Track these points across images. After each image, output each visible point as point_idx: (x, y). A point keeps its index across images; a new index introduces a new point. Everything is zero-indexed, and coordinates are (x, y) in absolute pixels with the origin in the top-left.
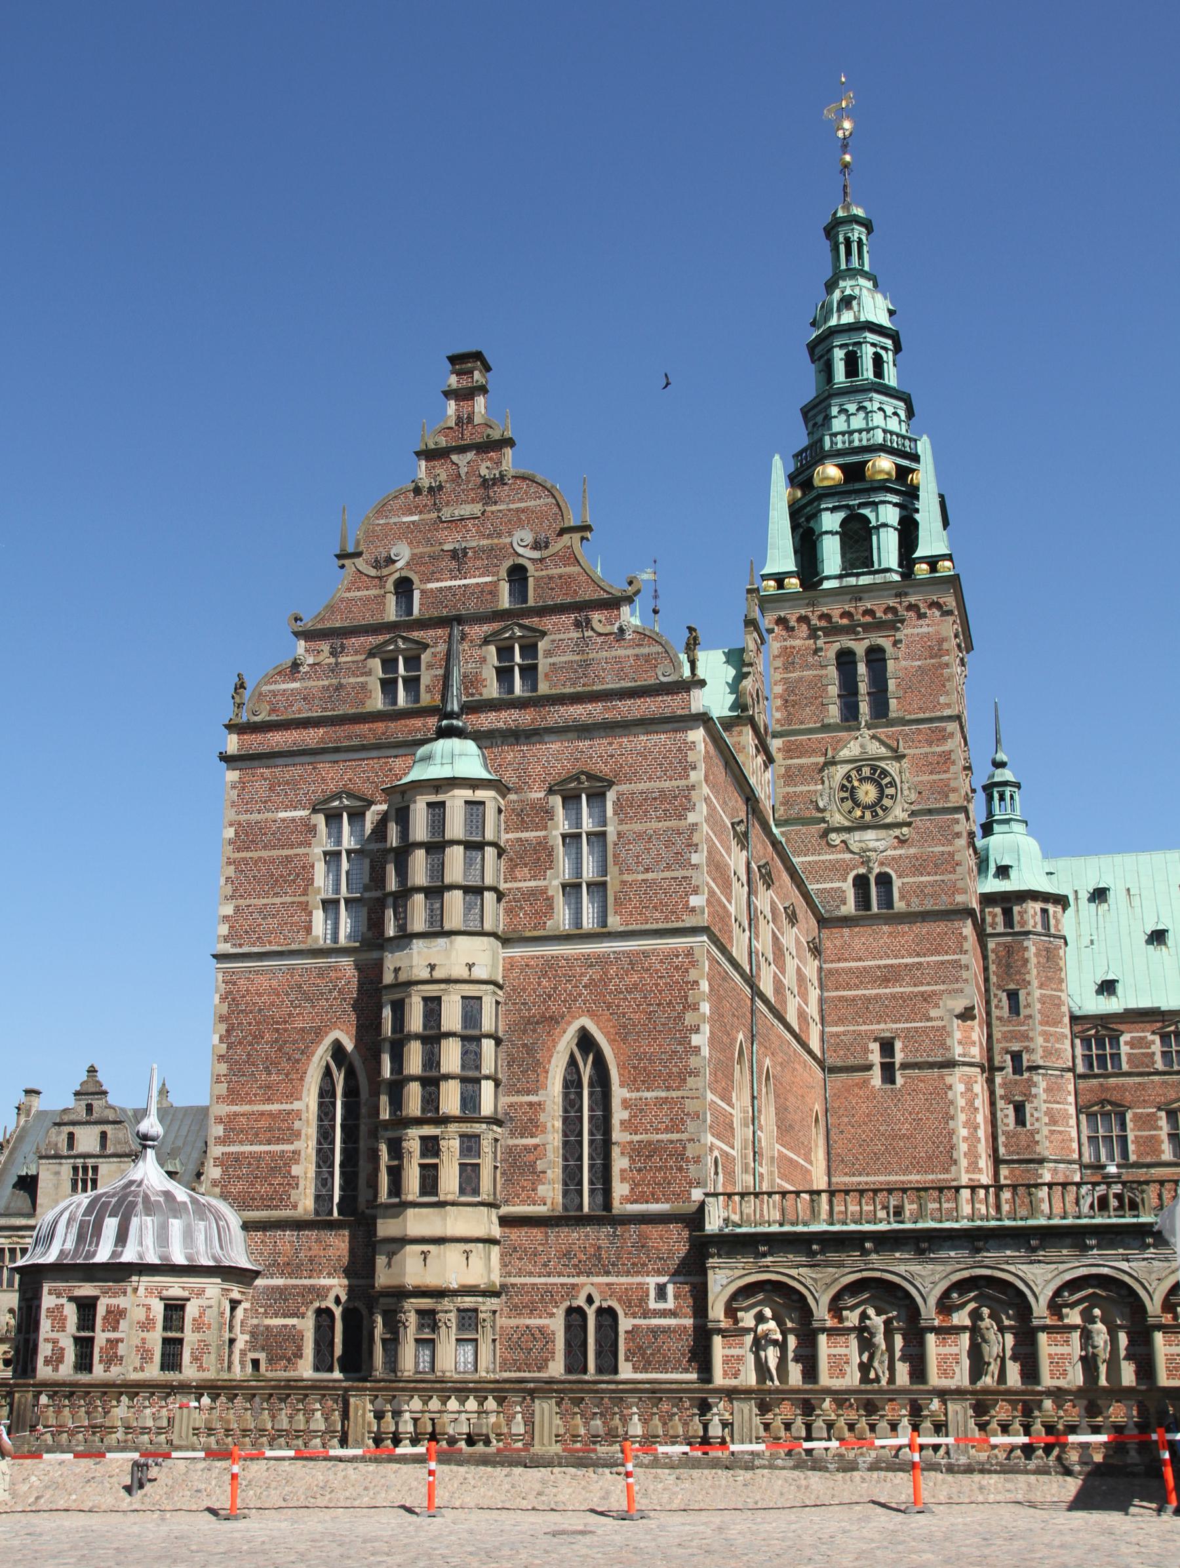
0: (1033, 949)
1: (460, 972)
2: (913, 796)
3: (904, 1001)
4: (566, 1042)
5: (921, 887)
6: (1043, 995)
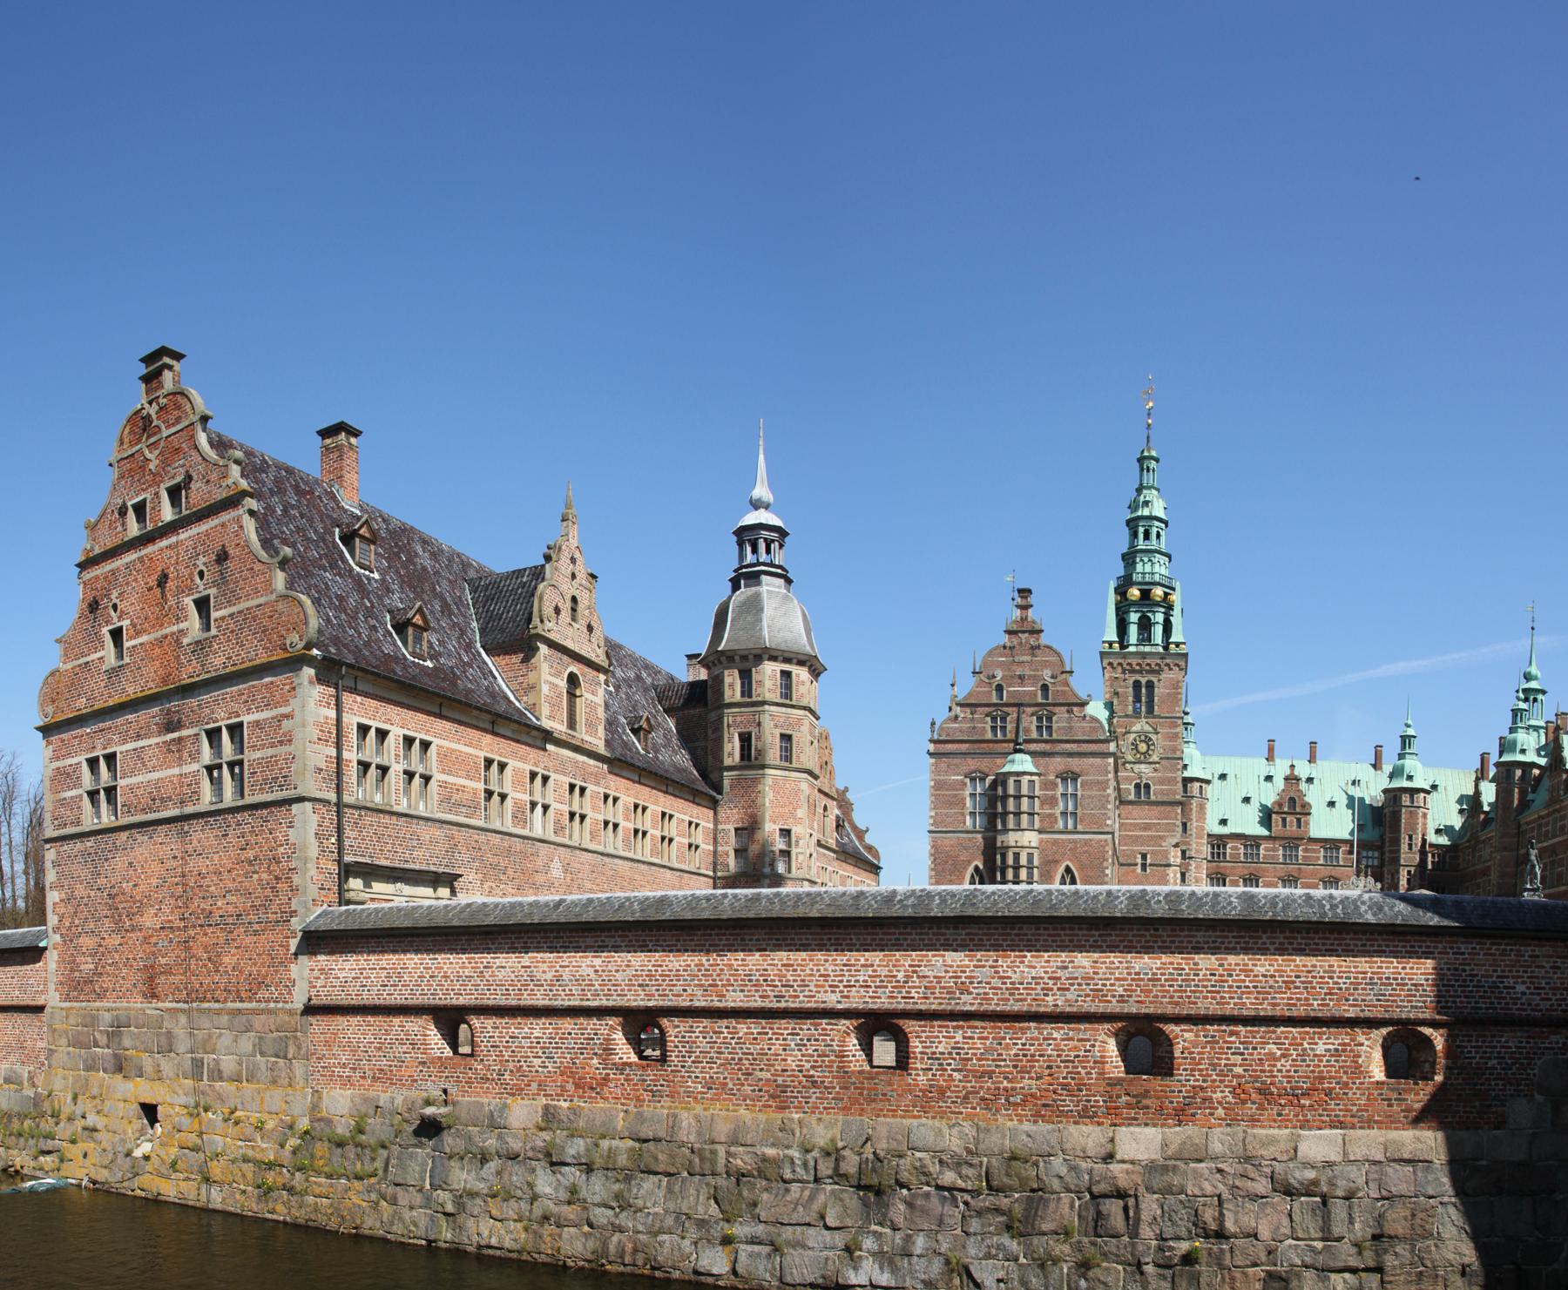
1: (1027, 844)
2: (1162, 751)
4: (1061, 870)
5: (1162, 790)
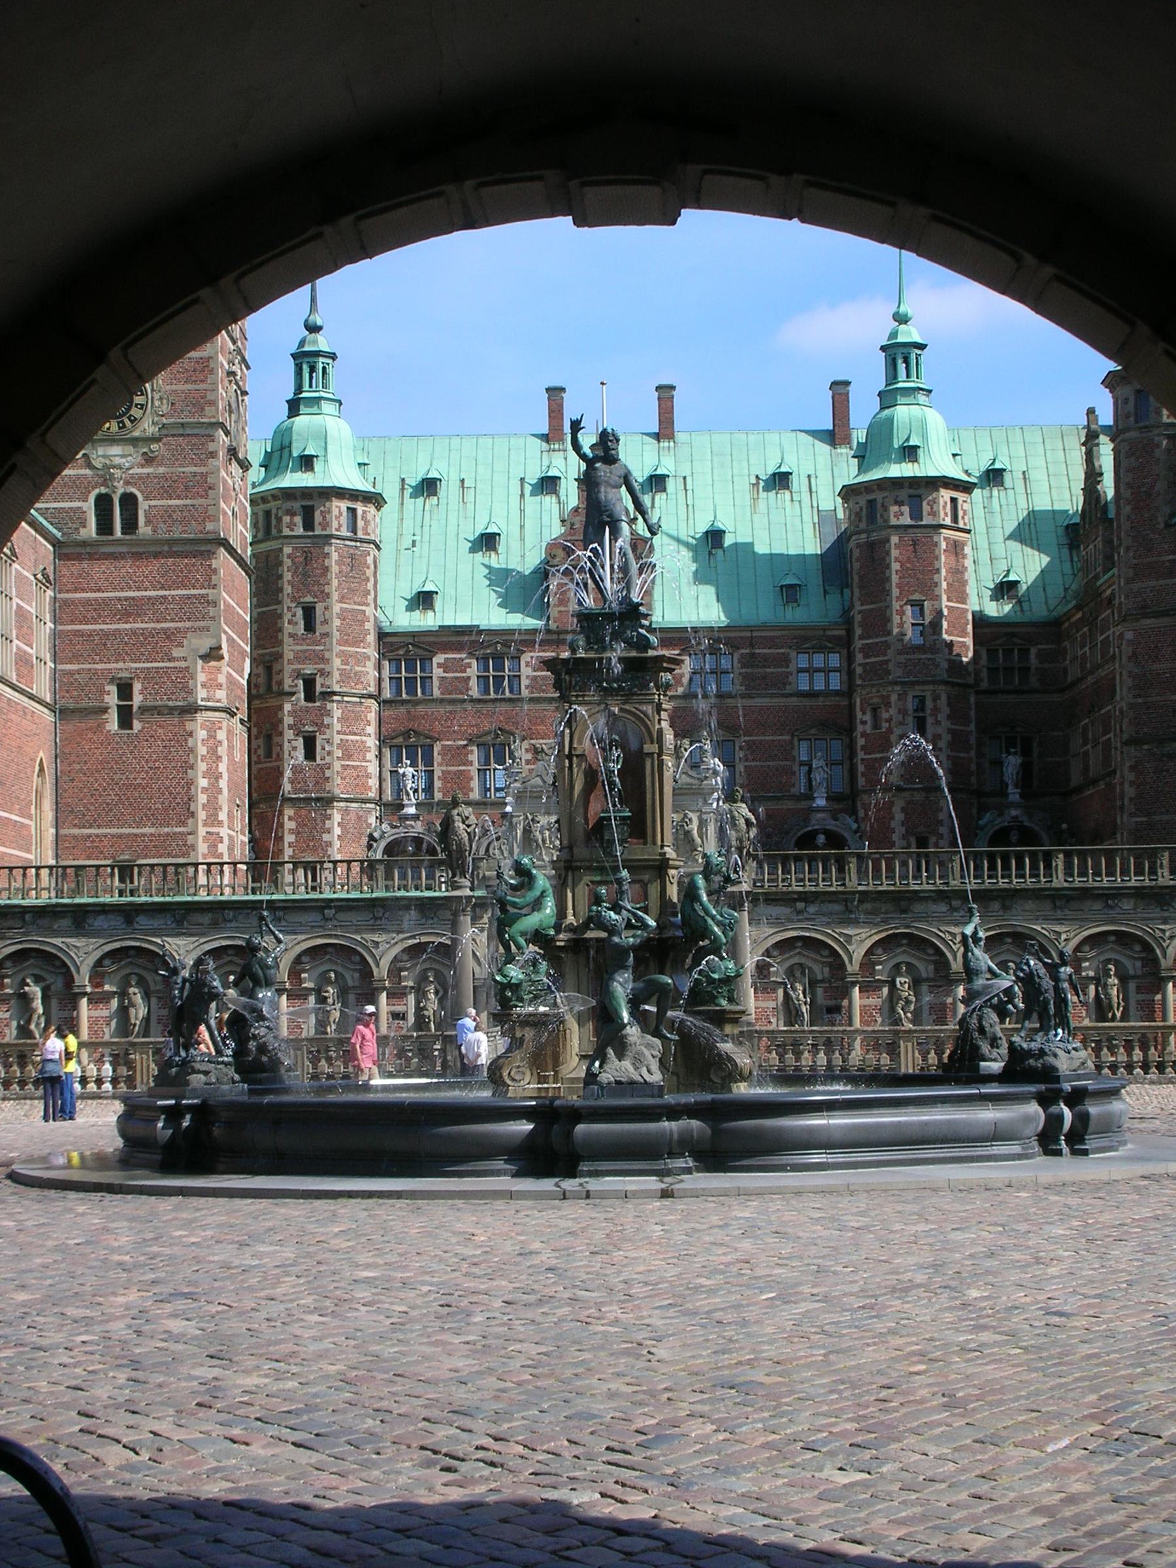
0: (335, 556)
2: (165, 408)
3: (145, 639)
5: (168, 512)
6: (341, 608)
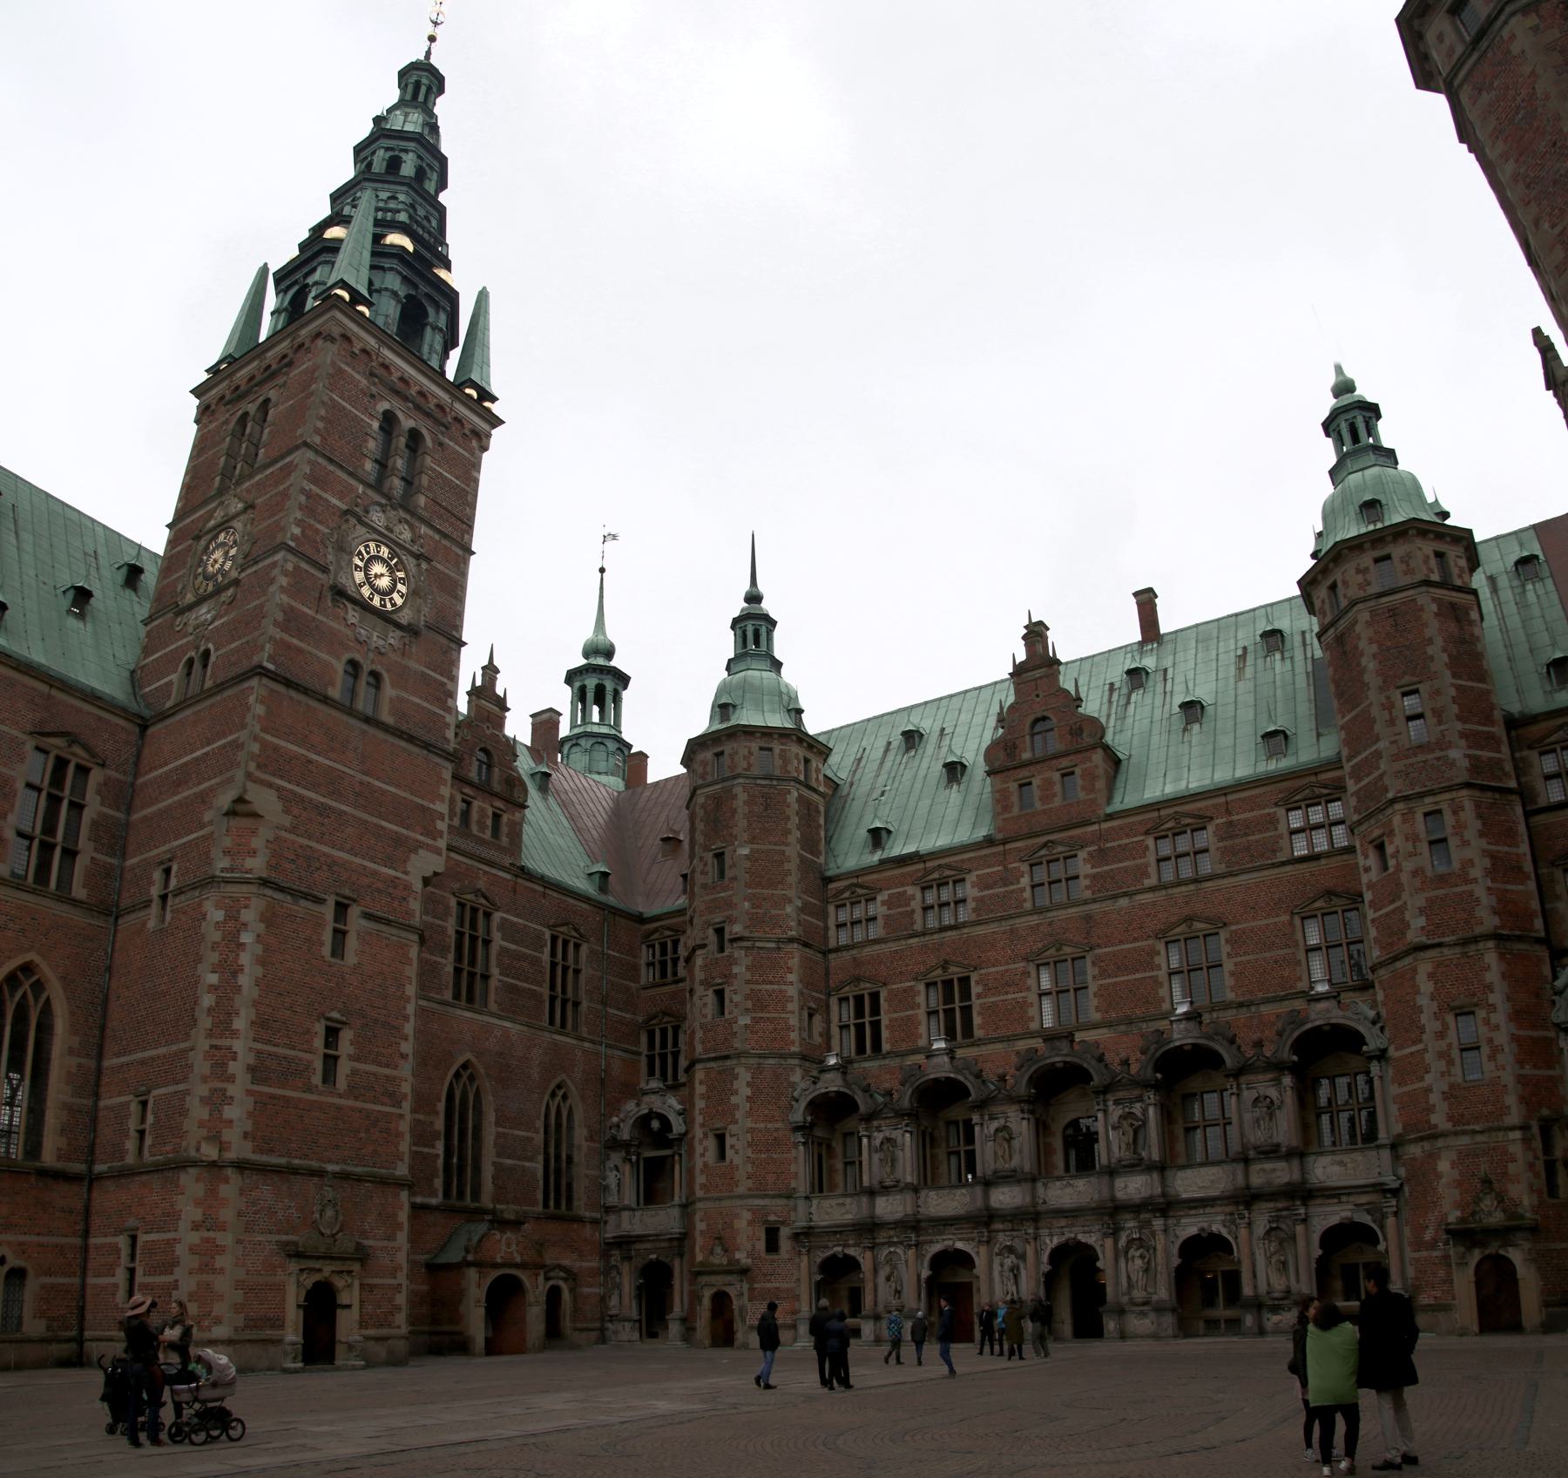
0: (742, 797)
